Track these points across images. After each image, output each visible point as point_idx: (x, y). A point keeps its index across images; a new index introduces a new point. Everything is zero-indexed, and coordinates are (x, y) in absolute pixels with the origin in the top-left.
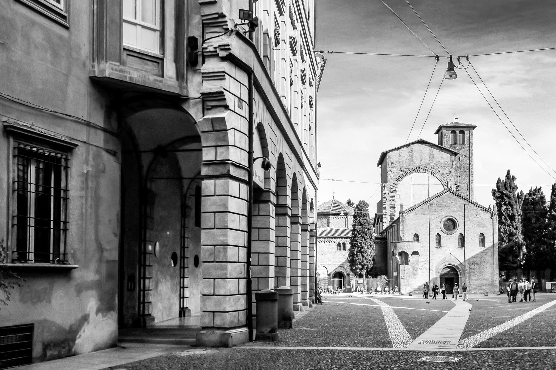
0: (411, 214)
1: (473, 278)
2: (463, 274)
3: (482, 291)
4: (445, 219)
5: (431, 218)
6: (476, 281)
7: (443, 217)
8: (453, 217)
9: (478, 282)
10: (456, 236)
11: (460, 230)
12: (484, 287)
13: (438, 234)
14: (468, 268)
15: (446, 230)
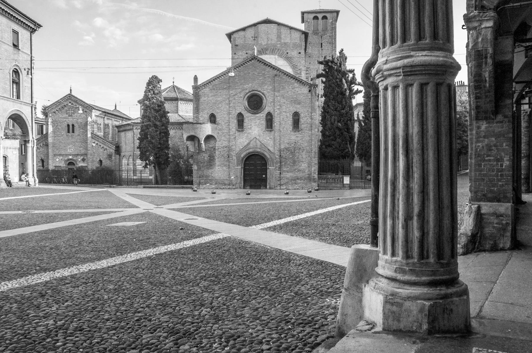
0: (206, 90)
1: (285, 169)
2: (272, 164)
3: (296, 186)
4: (248, 94)
5: (232, 93)
6: (288, 172)
7: (247, 92)
8: (259, 91)
9: (291, 174)
10: (262, 115)
11: (268, 108)
12: (299, 181)
13: (240, 115)
14: (277, 157)
15: (252, 109)
